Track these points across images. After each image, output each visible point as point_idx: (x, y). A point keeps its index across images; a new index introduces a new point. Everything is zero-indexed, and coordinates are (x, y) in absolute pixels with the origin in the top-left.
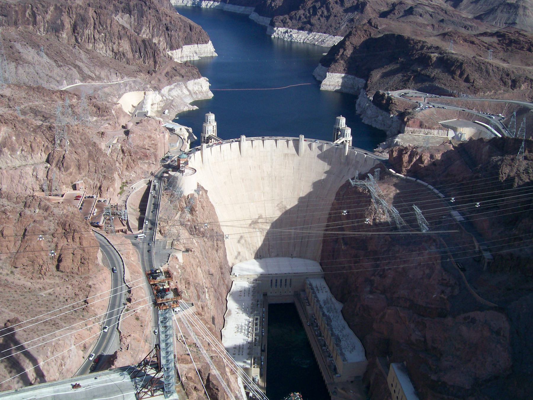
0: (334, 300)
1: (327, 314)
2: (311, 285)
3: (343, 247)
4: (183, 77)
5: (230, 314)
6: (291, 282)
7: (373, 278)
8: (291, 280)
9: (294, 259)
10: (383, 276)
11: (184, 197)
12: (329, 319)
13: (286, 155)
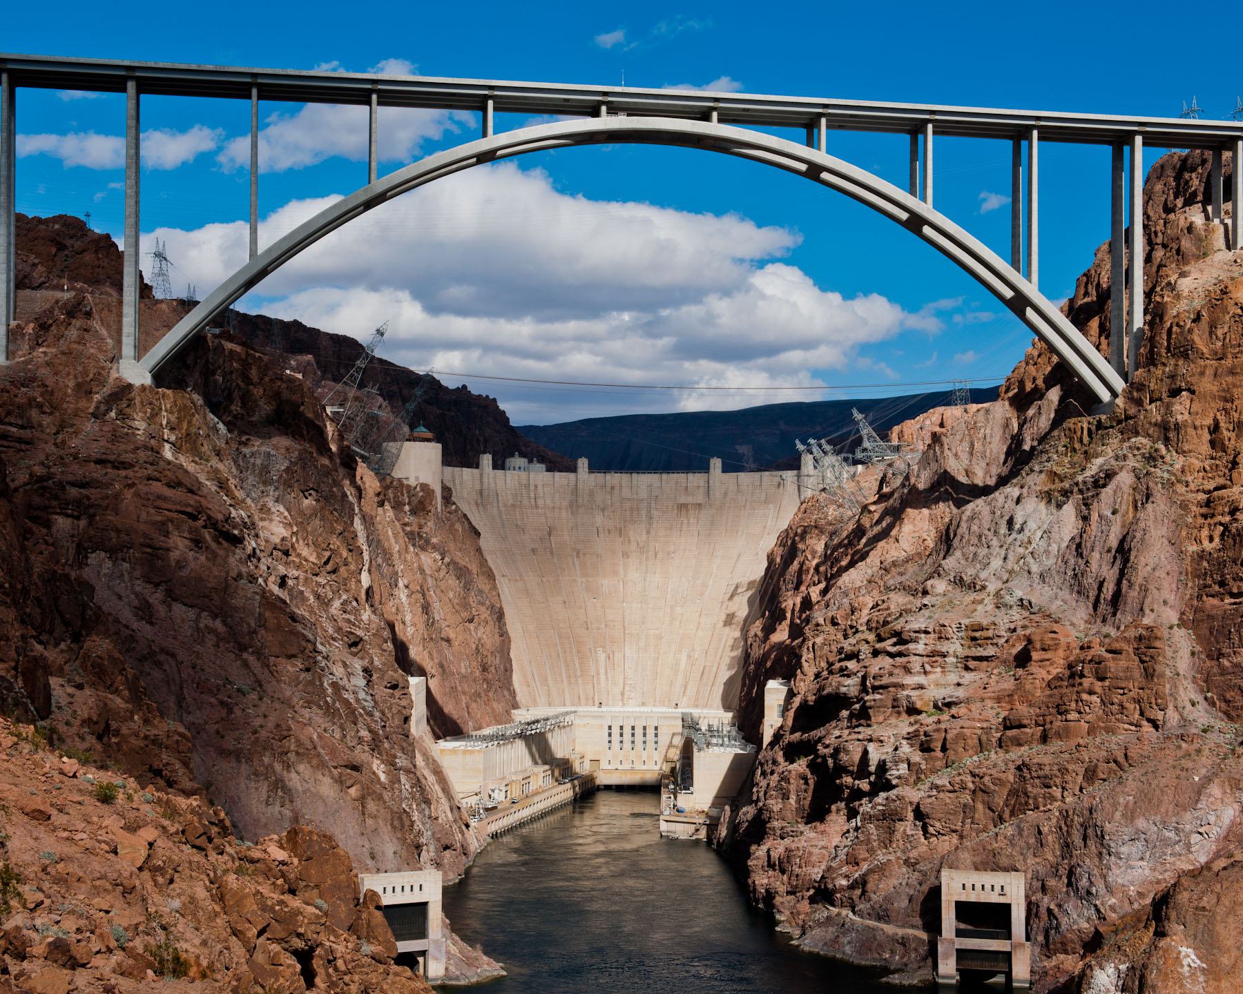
6: (656, 735)
8: (656, 728)
11: (409, 486)
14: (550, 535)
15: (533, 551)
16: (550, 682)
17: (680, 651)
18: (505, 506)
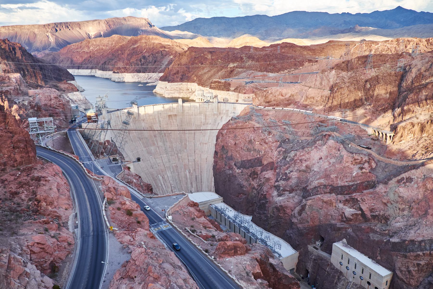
0: (241, 215)
1: (242, 225)
2: (216, 208)
3: (237, 171)
4: (64, 91)
7: (277, 184)
9: (193, 193)
10: (287, 179)
13: (170, 116)
17: (185, 171)
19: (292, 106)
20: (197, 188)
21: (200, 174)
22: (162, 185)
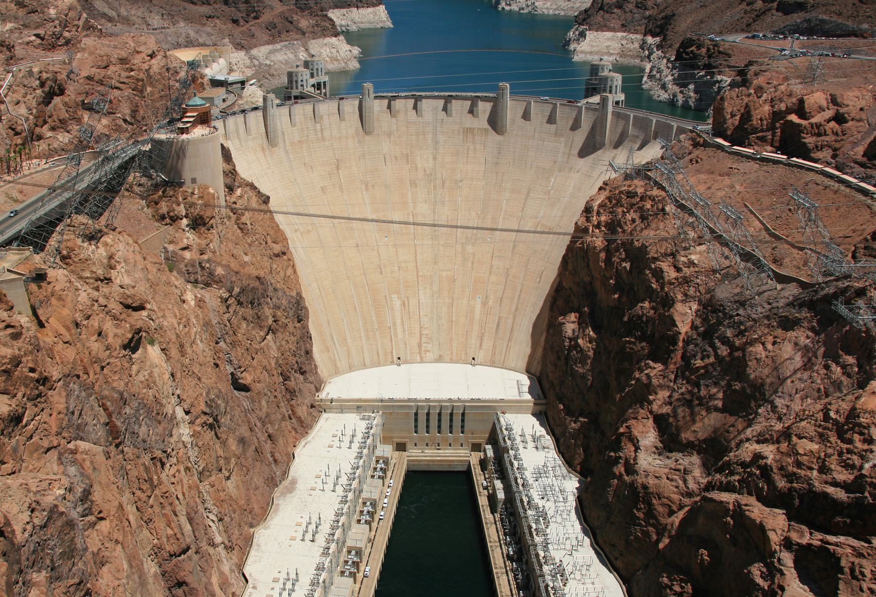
1: (541, 503)
5: (291, 489)
6: (463, 421)
12: (543, 515)
13: (468, 131)
14: (338, 169)
15: (323, 189)
16: (349, 341)
18: (292, 144)
19: (826, 154)
20: (494, 354)
21: (511, 316)
22: (395, 324)
